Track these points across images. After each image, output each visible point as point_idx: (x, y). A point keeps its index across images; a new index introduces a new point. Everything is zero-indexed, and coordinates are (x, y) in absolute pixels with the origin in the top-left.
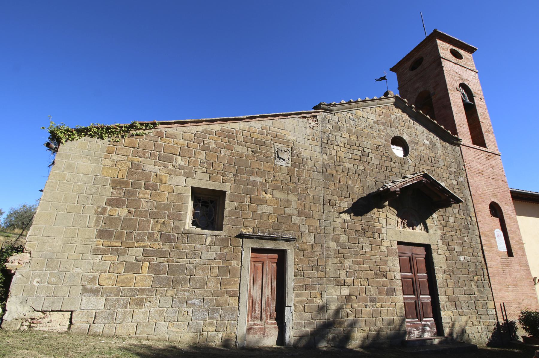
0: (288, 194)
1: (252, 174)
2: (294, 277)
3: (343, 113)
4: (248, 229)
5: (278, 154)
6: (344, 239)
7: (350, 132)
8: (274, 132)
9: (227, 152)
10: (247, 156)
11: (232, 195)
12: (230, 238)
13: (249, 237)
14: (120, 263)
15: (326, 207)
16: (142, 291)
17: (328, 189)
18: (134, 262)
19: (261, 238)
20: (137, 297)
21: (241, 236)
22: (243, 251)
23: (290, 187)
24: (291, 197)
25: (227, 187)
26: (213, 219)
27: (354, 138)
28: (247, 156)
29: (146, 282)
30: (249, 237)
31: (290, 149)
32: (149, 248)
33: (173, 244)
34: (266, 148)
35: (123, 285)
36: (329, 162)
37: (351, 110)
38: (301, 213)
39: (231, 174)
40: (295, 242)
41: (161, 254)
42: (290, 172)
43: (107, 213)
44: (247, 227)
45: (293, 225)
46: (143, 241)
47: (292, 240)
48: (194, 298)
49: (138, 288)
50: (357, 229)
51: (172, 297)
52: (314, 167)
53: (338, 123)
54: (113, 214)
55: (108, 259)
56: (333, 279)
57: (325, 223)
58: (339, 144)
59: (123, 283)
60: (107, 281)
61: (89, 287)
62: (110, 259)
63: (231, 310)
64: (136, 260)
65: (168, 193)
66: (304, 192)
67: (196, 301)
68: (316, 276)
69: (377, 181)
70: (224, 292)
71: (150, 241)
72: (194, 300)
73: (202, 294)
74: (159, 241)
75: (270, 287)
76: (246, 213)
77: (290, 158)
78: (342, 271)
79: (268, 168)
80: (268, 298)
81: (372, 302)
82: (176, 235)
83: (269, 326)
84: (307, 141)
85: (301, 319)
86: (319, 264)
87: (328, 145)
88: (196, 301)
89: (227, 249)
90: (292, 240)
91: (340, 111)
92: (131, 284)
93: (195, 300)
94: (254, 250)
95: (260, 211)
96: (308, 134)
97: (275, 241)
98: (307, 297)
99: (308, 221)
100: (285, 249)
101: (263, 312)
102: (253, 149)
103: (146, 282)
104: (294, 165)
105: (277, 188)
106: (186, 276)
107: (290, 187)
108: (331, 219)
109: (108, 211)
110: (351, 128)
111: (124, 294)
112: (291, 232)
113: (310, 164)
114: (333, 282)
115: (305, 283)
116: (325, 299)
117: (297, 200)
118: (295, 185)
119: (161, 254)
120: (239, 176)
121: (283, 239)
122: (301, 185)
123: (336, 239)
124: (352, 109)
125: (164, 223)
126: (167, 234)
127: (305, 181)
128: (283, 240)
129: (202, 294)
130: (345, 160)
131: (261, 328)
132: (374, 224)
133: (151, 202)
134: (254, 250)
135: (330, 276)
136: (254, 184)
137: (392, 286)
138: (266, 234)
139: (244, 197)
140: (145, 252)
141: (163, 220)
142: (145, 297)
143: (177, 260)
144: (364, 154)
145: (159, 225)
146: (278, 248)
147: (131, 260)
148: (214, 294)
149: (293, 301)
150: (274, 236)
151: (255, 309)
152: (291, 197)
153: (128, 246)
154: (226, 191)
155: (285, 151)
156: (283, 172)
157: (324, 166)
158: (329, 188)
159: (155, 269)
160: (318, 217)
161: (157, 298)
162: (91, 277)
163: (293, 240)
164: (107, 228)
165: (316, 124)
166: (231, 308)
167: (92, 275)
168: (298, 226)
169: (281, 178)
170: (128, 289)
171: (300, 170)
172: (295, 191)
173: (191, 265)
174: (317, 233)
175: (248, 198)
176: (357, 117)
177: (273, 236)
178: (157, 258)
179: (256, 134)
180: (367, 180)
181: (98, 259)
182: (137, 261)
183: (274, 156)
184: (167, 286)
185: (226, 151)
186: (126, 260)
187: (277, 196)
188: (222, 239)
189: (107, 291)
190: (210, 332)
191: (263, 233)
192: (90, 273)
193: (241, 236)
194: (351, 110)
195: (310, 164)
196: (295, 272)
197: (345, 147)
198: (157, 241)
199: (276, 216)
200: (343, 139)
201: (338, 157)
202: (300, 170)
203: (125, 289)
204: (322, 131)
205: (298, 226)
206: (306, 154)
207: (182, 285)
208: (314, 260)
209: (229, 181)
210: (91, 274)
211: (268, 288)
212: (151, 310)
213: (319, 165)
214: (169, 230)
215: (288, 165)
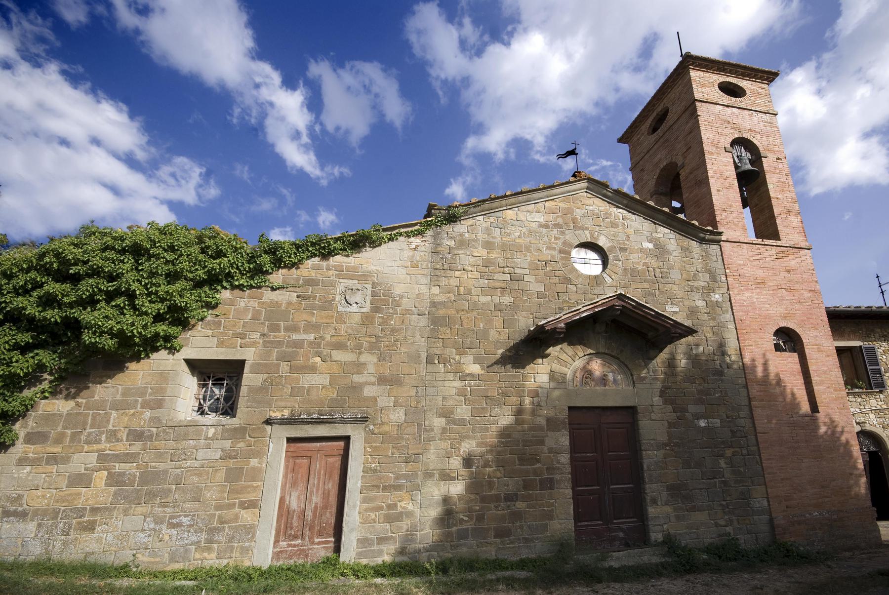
0: (360, 353)
1: (295, 329)
2: (362, 474)
3: (477, 218)
4: (282, 411)
5: (345, 295)
6: (463, 411)
7: (488, 246)
8: (341, 263)
9: (252, 302)
10: (289, 304)
11: (252, 366)
12: (248, 426)
13: (283, 422)
14: (59, 475)
15: (430, 366)
16: (95, 510)
17: (437, 340)
18: (83, 471)
19: (304, 422)
20: (86, 519)
21: (268, 422)
22: (271, 443)
23: (365, 342)
24: (365, 358)
25: (249, 355)
26: (234, 401)
27: (495, 255)
28: (289, 304)
29: (101, 499)
30: (283, 422)
31: (369, 287)
32: (108, 452)
33: (149, 442)
34: (323, 289)
35: (64, 504)
36: (442, 298)
37: (493, 211)
38: (382, 380)
39: (256, 335)
40: (368, 423)
41: (128, 458)
42: (367, 319)
43: (40, 409)
44: (281, 409)
45: (366, 399)
46: (99, 442)
47: (361, 421)
48: (180, 516)
49: (88, 507)
50: (489, 395)
51: (143, 517)
52: (414, 309)
53: (466, 235)
54: (49, 410)
55: (41, 471)
56: (435, 472)
57: (427, 391)
58: (466, 268)
59: (64, 502)
60: (39, 500)
61: (12, 509)
62: (44, 471)
63: (245, 528)
64: (86, 469)
65: (142, 372)
66: (391, 348)
67: (184, 520)
68: (404, 470)
69: (536, 318)
70: (234, 504)
71: (109, 442)
72: (181, 518)
73: (194, 509)
74: (125, 440)
75: (320, 492)
76: (280, 389)
77: (369, 299)
78: (454, 459)
79: (326, 318)
80: (316, 507)
81: (510, 501)
82: (154, 430)
83: (316, 546)
84: (404, 271)
85: (371, 533)
86: (410, 452)
87: (442, 271)
88: (184, 520)
89: (242, 443)
90: (361, 421)
91: (471, 216)
92: (76, 503)
93: (182, 518)
94: (290, 440)
95: (307, 383)
96: (406, 259)
97: (329, 425)
98: (384, 501)
99: (395, 390)
100: (349, 434)
101: (306, 527)
102: (299, 294)
103: (101, 499)
104: (376, 309)
105: (340, 346)
106: (168, 485)
107: (365, 342)
108: (440, 384)
109: (41, 406)
110: (491, 240)
111: (66, 516)
112: (362, 409)
113: (406, 303)
114: (437, 476)
115: (383, 481)
116: (419, 501)
117: (375, 360)
118: (374, 340)
119: (128, 458)
120: (270, 335)
121: (343, 421)
122: (385, 337)
123: (446, 413)
124: (495, 210)
125: (134, 414)
126: (138, 429)
127: (393, 331)
128: (345, 421)
129: (194, 509)
130: (475, 291)
131: (300, 550)
132: (523, 384)
133: (113, 387)
134: (290, 440)
135: (431, 468)
136: (298, 344)
137: (553, 474)
138: (315, 416)
139: (279, 365)
140: (103, 457)
141: (132, 411)
142: (99, 518)
143: (153, 464)
144: (515, 278)
145: (126, 419)
146: (335, 435)
147: (78, 470)
148: (218, 507)
149: (358, 508)
150: (326, 417)
151: (291, 524)
152: (365, 358)
153: (72, 450)
154: (245, 360)
155: (358, 289)
156: (353, 322)
157: (434, 304)
158: (439, 338)
159: (114, 480)
160: (414, 383)
161: (119, 519)
162: (15, 496)
163: (364, 420)
164: (40, 430)
165: (423, 241)
166: (246, 525)
167: (16, 494)
168: (375, 399)
169: (350, 331)
170: (71, 509)
171: (385, 315)
172: (373, 348)
173: (179, 470)
174: (411, 407)
175: (285, 367)
176: (504, 221)
177: (325, 417)
178: (121, 464)
179: (307, 270)
180: (516, 317)
181: (25, 471)
182: (88, 470)
183: (337, 299)
184: (136, 502)
185: (249, 302)
186: (69, 470)
187: (338, 359)
188: (235, 429)
189: (40, 513)
190: (206, 559)
191: (309, 414)
192: (14, 490)
193: (268, 422)
194: (493, 211)
195: (406, 303)
196: (364, 467)
197: (477, 271)
198: (122, 440)
199: (335, 388)
200: (472, 260)
201: (462, 289)
202: (385, 315)
203: (66, 509)
204: (433, 251)
205: (375, 399)
206: (398, 290)
207: (160, 499)
208: (401, 446)
209: (254, 344)
210: (16, 492)
211: (317, 492)
212: (108, 536)
213: (425, 306)
214: (142, 423)
215: (363, 310)
